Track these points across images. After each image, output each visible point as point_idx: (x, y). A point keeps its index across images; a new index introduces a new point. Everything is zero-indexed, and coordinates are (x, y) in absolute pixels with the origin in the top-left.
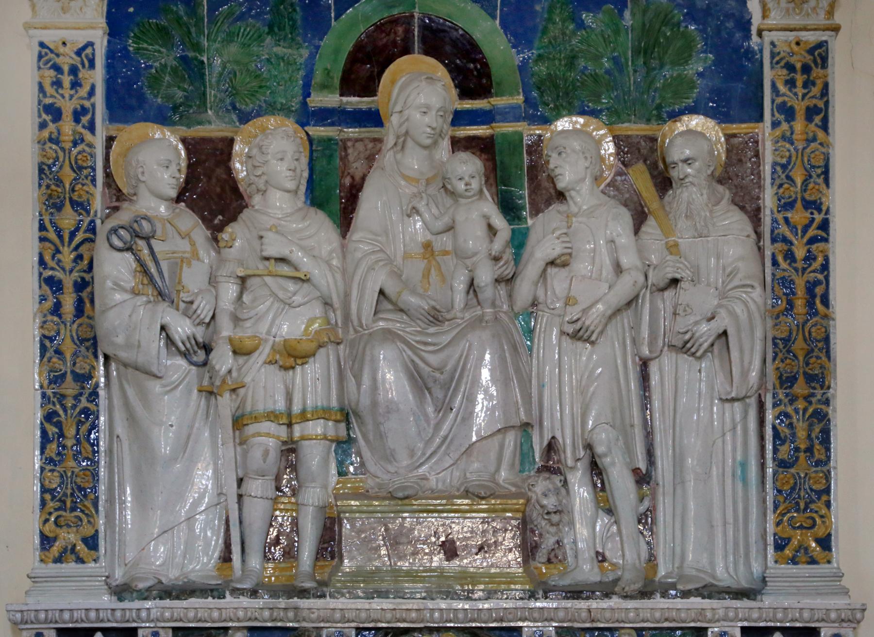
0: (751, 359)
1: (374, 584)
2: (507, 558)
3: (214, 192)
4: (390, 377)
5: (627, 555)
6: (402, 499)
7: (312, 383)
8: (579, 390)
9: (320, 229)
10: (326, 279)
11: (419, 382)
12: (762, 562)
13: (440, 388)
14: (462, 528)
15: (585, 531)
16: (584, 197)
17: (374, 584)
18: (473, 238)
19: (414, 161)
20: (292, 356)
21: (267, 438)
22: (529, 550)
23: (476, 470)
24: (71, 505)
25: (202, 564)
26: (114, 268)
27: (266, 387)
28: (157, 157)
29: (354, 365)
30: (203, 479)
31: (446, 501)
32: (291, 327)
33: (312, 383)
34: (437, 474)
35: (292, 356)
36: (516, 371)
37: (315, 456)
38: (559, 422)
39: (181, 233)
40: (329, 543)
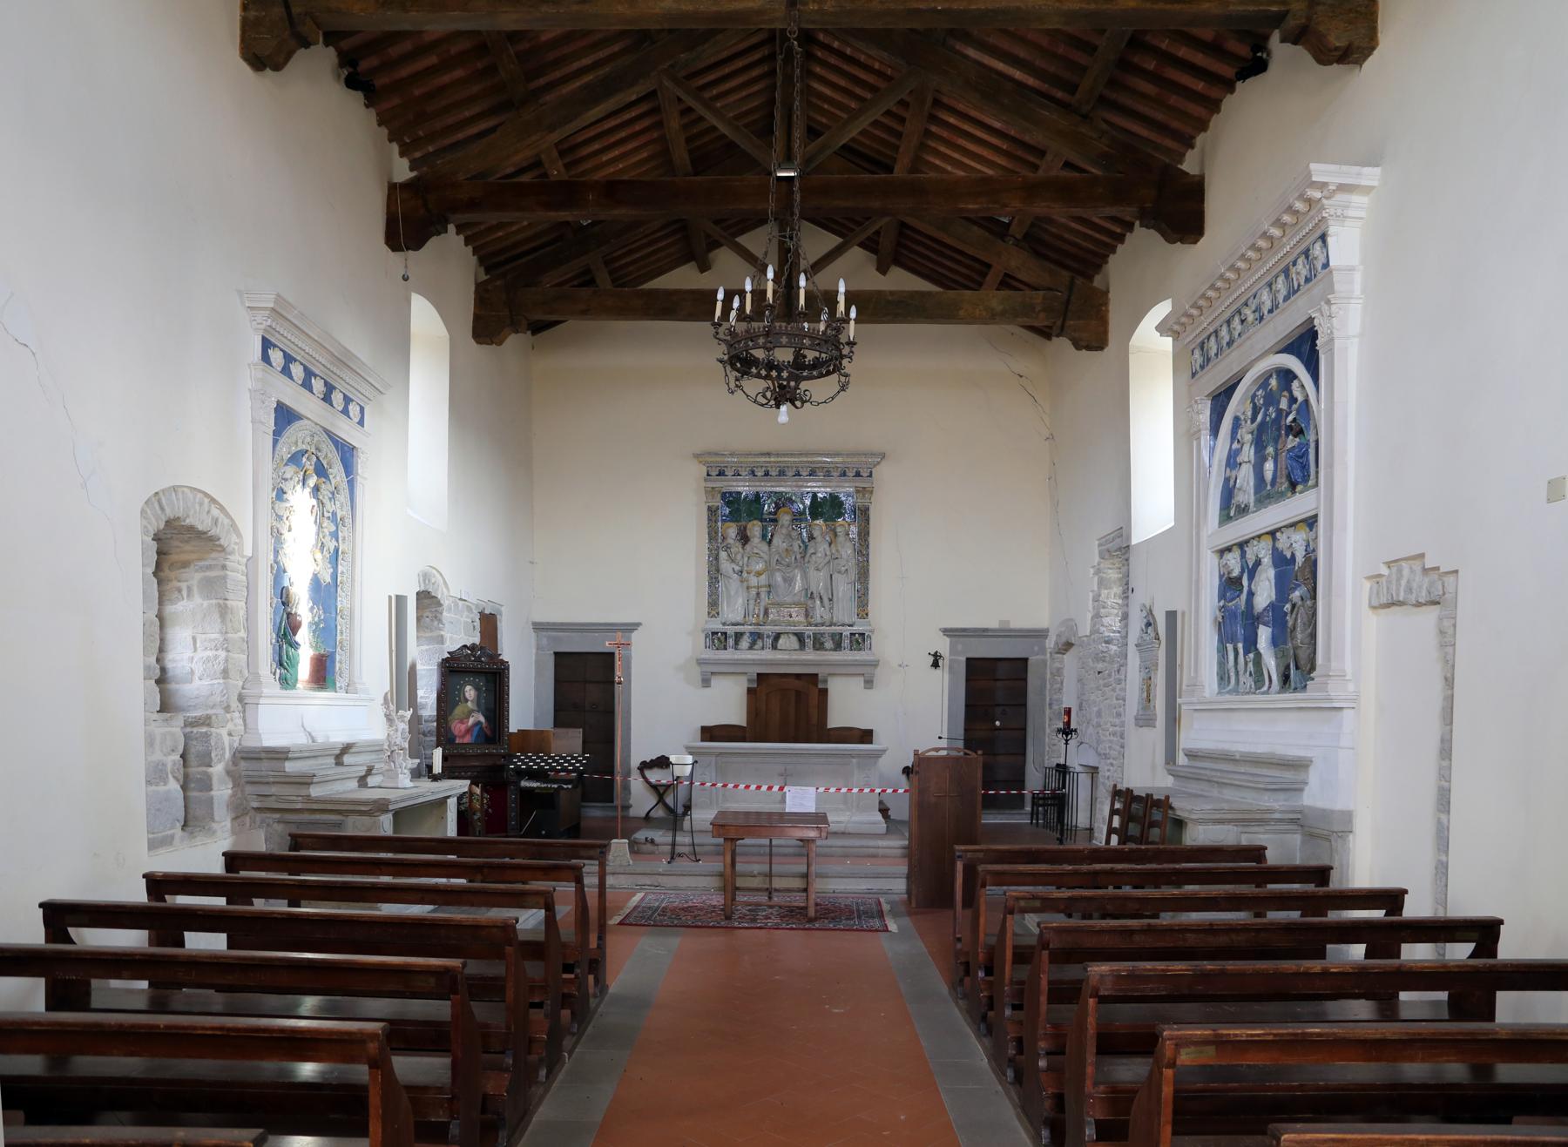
0: (853, 575)
1: (775, 623)
2: (802, 619)
3: (744, 538)
4: (779, 578)
5: (827, 617)
6: (779, 605)
7: (763, 579)
8: (818, 581)
9: (765, 547)
10: (766, 557)
11: (785, 580)
12: (855, 618)
13: (789, 581)
14: (794, 611)
15: (819, 612)
16: (819, 539)
17: (775, 623)
18: (796, 548)
19: (784, 531)
20: (759, 574)
21: (754, 591)
22: (807, 616)
23: (796, 599)
24: (713, 604)
25: (739, 618)
26: (723, 555)
27: (754, 581)
28: (732, 531)
29: (771, 576)
30: (740, 601)
31: (790, 605)
32: (760, 566)
33: (763, 579)
34: (788, 599)
35: (759, 574)
36: (805, 577)
37: (763, 595)
38: (813, 588)
39: (736, 548)
40: (766, 613)
